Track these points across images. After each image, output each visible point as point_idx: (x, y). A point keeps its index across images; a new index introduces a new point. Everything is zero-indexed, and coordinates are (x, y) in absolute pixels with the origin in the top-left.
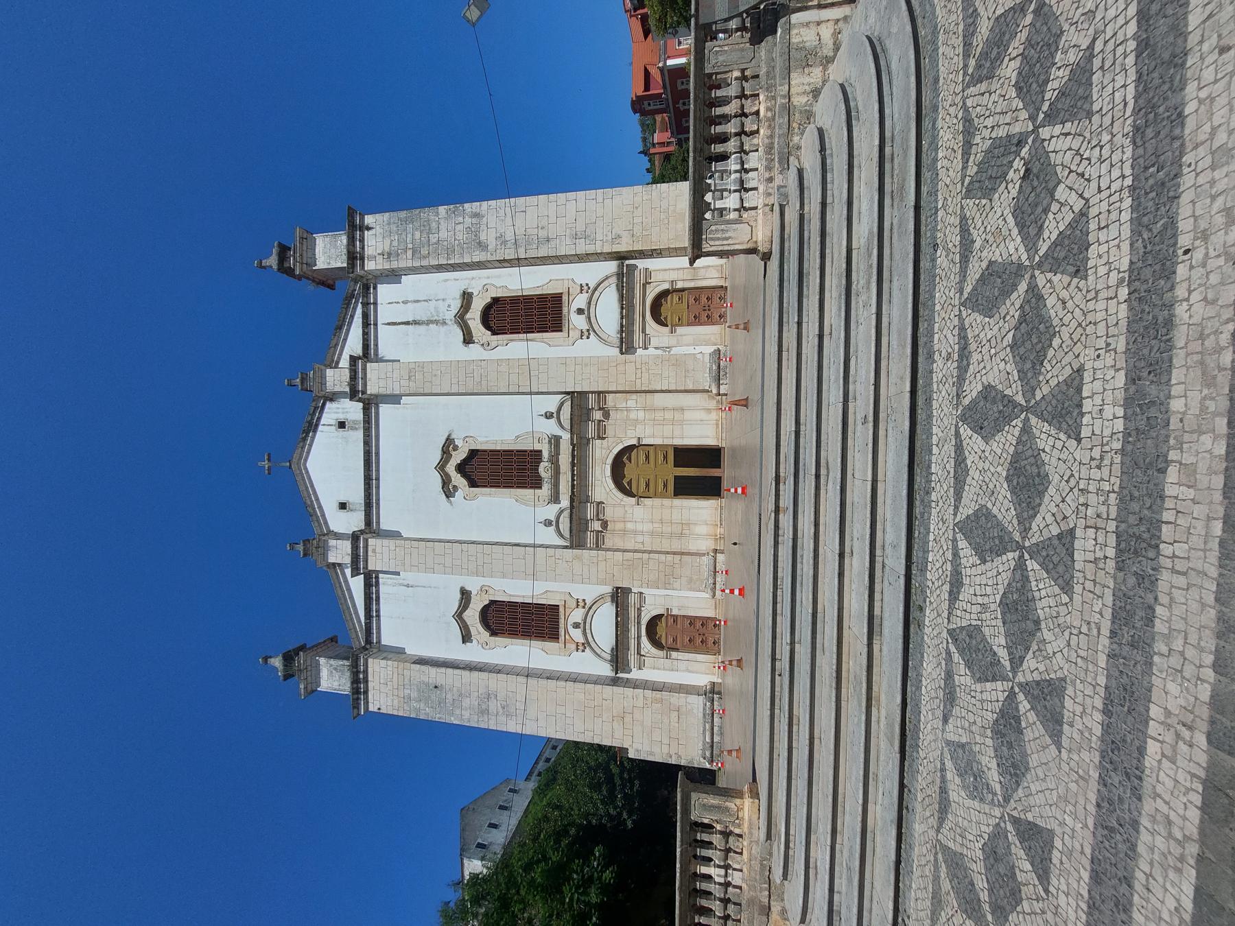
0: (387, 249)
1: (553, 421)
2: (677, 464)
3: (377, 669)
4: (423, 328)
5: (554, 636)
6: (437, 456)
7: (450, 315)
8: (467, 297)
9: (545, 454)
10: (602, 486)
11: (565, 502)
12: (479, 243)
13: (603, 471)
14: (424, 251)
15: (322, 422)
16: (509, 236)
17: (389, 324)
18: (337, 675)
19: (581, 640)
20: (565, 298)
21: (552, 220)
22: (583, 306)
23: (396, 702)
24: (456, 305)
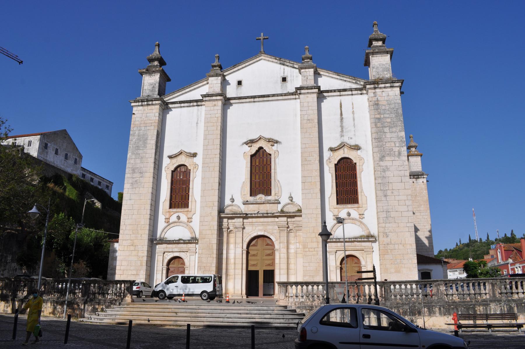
0: (380, 103)
2: (265, 272)
3: (154, 111)
4: (338, 123)
6: (268, 136)
7: (346, 139)
8: (357, 148)
9: (269, 198)
11: (244, 209)
12: (384, 156)
13: (260, 230)
14: (379, 125)
15: (286, 67)
16: (388, 174)
17: (341, 104)
18: (150, 88)
19: (171, 221)
20: (356, 205)
21: (397, 198)
22: (352, 216)
23: (137, 123)
24: (352, 143)
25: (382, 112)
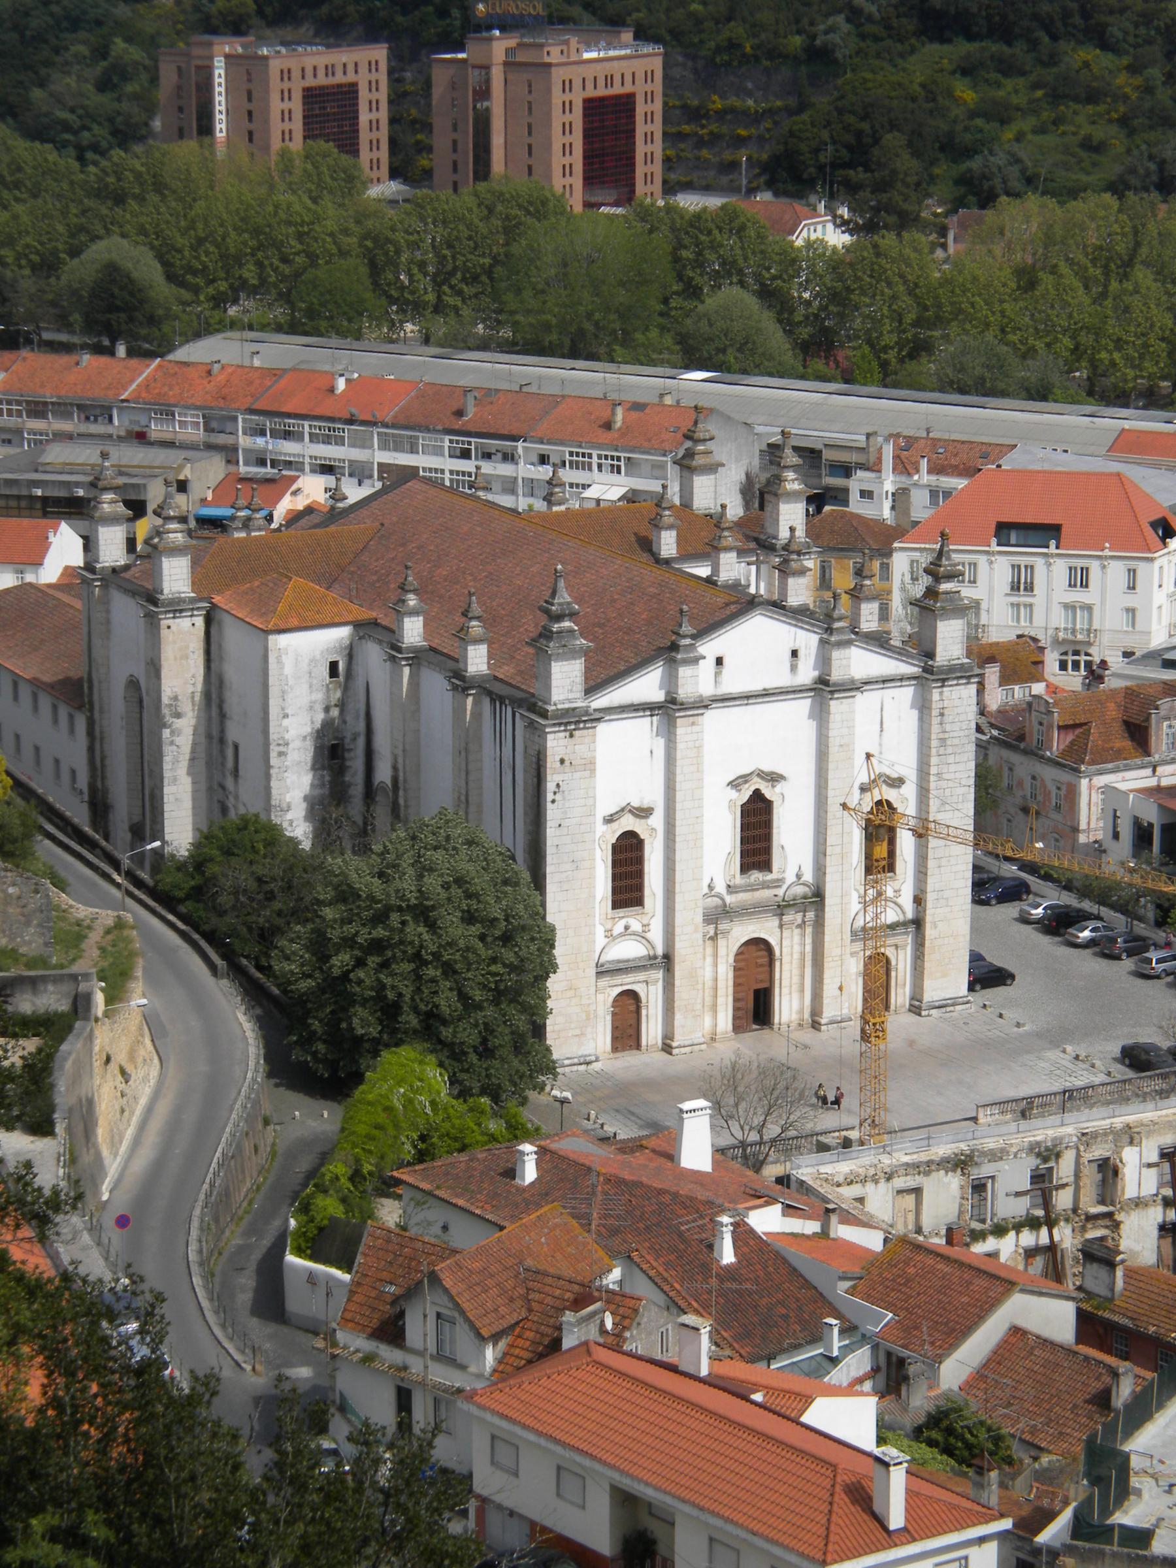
1: (794, 879)
5: (616, 905)
6: (767, 767)
9: (769, 877)
10: (741, 932)
15: (799, 631)
25: (948, 727)
